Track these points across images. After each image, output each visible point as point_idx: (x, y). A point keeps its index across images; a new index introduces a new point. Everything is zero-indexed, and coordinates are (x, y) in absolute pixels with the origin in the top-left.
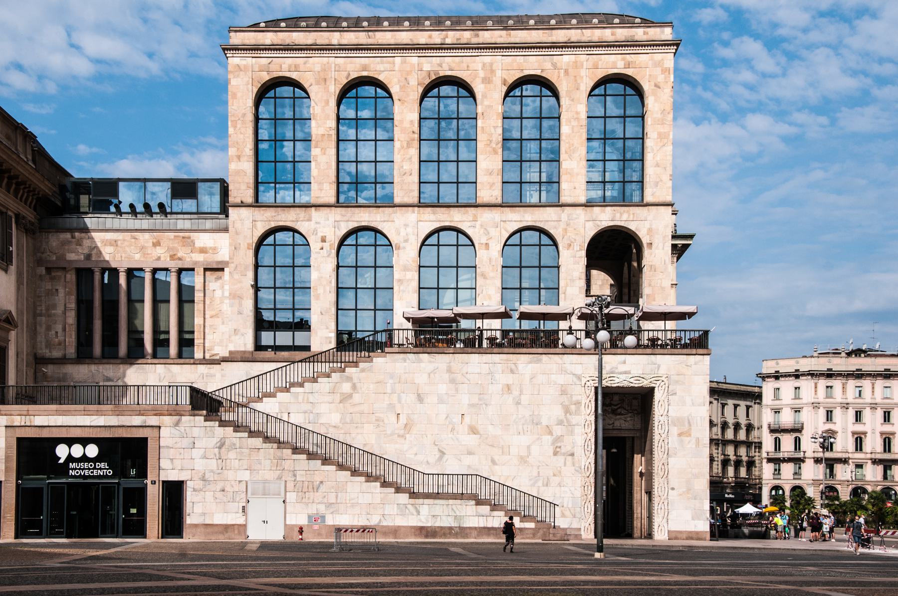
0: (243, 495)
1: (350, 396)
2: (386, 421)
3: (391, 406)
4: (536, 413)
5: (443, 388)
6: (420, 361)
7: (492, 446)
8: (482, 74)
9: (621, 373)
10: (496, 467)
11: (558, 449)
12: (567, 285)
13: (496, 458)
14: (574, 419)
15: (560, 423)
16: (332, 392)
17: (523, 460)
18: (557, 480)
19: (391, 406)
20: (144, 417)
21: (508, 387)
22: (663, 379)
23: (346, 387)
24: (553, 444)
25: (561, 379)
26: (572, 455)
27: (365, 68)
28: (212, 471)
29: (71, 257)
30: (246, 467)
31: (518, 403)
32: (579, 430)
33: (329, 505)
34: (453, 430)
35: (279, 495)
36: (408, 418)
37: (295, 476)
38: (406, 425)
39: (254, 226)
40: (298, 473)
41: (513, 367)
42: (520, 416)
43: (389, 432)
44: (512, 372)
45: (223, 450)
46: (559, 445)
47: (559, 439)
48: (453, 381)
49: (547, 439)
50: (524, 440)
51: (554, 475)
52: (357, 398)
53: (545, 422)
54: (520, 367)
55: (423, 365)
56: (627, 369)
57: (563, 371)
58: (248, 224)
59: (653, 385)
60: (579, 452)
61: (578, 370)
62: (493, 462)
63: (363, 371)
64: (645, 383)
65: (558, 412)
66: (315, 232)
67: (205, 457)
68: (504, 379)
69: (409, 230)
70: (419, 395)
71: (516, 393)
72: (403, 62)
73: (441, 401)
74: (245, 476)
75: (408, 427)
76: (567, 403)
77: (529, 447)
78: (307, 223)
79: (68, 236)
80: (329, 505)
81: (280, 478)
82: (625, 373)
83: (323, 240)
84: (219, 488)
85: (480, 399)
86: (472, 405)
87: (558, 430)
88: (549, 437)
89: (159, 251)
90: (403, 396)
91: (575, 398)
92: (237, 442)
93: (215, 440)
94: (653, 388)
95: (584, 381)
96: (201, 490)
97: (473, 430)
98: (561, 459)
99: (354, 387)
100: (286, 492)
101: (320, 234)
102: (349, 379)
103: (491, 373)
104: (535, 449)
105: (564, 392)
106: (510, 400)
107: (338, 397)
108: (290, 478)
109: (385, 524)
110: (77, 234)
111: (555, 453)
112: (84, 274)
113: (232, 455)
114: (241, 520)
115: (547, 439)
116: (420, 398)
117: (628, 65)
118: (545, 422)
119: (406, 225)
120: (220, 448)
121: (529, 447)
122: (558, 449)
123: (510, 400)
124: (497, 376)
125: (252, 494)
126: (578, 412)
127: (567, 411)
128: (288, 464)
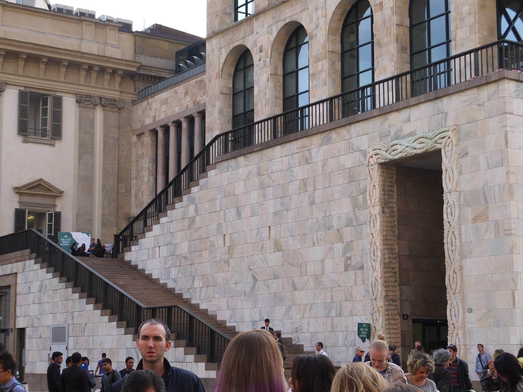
1: (193, 220)
2: (216, 246)
3: (219, 225)
4: (327, 215)
5: (254, 196)
6: (238, 167)
7: (292, 264)
9: (404, 137)
10: (296, 292)
11: (349, 262)
12: (457, 28)
13: (296, 280)
14: (363, 215)
17: (318, 278)
20: (10, 266)
21: (304, 182)
22: (450, 134)
24: (344, 253)
25: (348, 160)
26: (362, 268)
31: (312, 203)
32: (367, 230)
34: (262, 247)
35: (64, 340)
36: (232, 239)
37: (73, 318)
38: (229, 247)
39: (220, 53)
41: (308, 155)
42: (315, 220)
43: (218, 259)
44: (307, 162)
45: (42, 293)
46: (349, 255)
48: (262, 186)
49: (339, 247)
50: (316, 253)
51: (346, 300)
52: (198, 222)
53: (335, 226)
54: (314, 152)
56: (411, 129)
57: (351, 149)
58: (216, 52)
59: (438, 146)
60: (368, 264)
61: (363, 142)
64: (427, 146)
68: (300, 173)
69: (319, 13)
70: (238, 209)
71: (310, 189)
75: (230, 250)
76: (355, 194)
77: (323, 261)
78: (251, 36)
81: (66, 321)
82: (410, 134)
85: (282, 204)
86: (276, 213)
87: (348, 234)
88: (340, 244)
89: (188, 99)
91: (362, 184)
94: (439, 151)
95: (368, 156)
97: (278, 247)
98: (351, 274)
99: (196, 210)
100: (68, 337)
101: (259, 45)
103: (290, 168)
105: (351, 179)
107: (186, 222)
111: (346, 269)
116: (239, 214)
118: (335, 226)
119: (317, 9)
121: (323, 261)
122: (349, 262)
126: (365, 206)
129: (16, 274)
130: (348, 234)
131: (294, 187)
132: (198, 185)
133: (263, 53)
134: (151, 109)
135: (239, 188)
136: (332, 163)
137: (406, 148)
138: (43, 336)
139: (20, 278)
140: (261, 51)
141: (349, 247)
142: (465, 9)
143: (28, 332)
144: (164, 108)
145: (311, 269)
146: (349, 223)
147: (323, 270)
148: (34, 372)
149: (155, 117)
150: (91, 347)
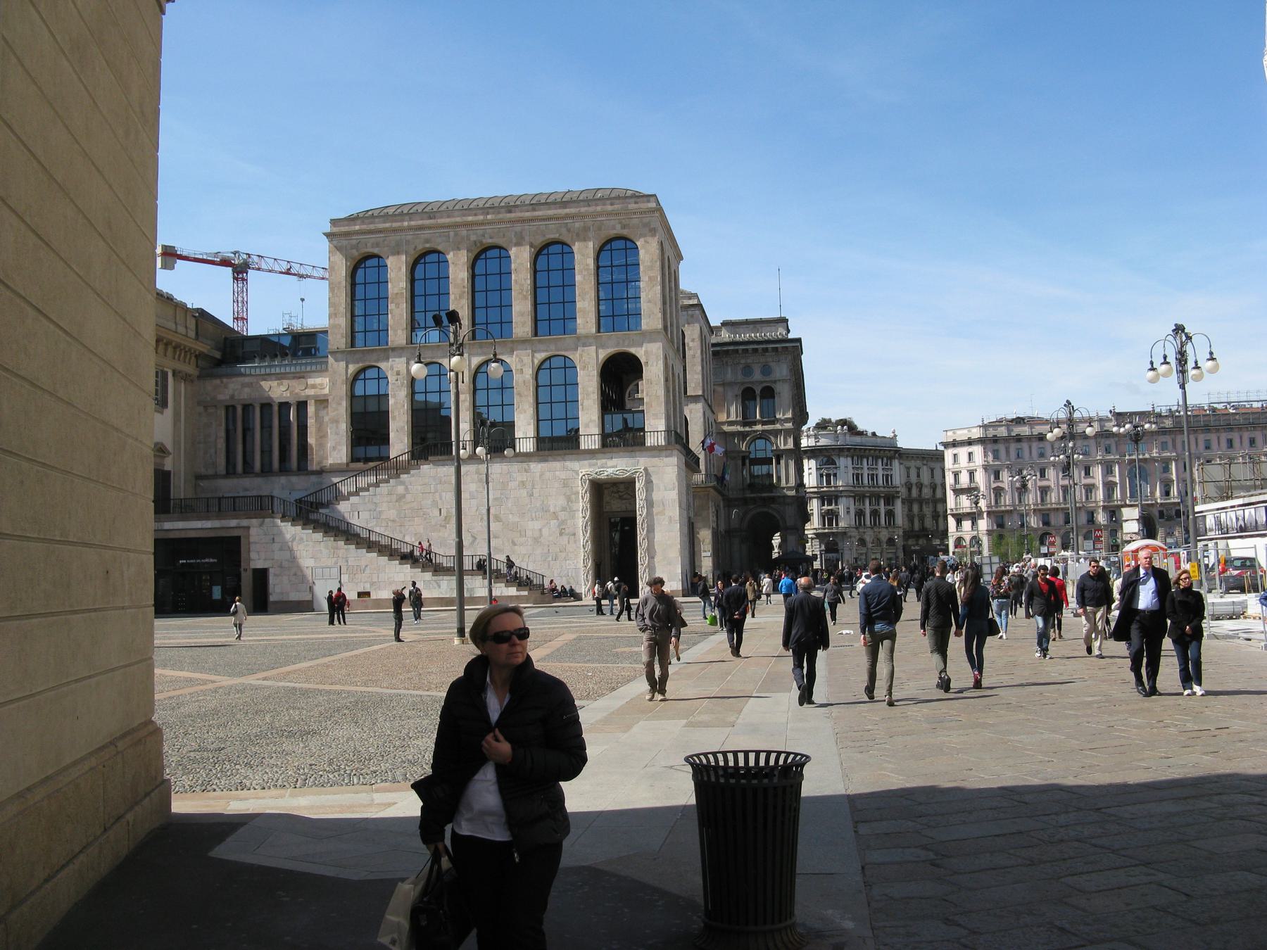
3: (435, 503)
8: (514, 240)
15: (564, 509)
16: (390, 494)
18: (563, 555)
19: (435, 503)
23: (401, 489)
25: (563, 475)
27: (427, 241)
29: (221, 397)
31: (532, 495)
44: (526, 471)
47: (563, 522)
49: (554, 523)
50: (537, 525)
52: (409, 497)
53: (552, 510)
56: (615, 466)
57: (565, 469)
62: (514, 544)
65: (562, 501)
66: (392, 368)
68: (520, 477)
72: (456, 235)
79: (218, 381)
80: (372, 584)
83: (398, 374)
87: (562, 515)
98: (565, 538)
99: (406, 489)
102: (403, 483)
104: (545, 532)
106: (524, 493)
107: (394, 498)
110: (225, 380)
111: (561, 534)
112: (230, 409)
115: (554, 523)
118: (552, 510)
123: (524, 493)
127: (569, 499)
128: (341, 553)
130: (562, 515)
134: (226, 387)
136: (548, 474)
139: (253, 531)
140: (398, 374)
141: (563, 522)
142: (591, 389)
143: (271, 571)
144: (247, 390)
145: (529, 533)
146: (564, 509)
147: (541, 535)
149: (232, 397)
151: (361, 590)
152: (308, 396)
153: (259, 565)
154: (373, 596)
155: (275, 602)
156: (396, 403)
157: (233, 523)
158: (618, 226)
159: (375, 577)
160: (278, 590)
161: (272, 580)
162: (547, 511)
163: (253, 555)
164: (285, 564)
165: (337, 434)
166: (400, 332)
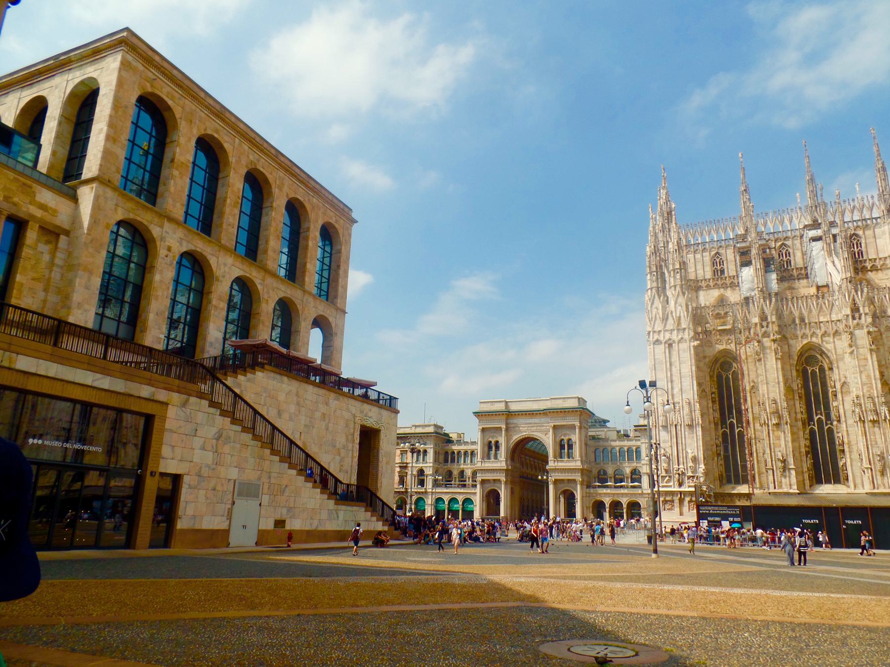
0: (230, 496)
5: (293, 408)
6: (282, 382)
20: (153, 389)
27: (217, 131)
28: (208, 466)
30: (235, 464)
31: (327, 429)
33: (290, 509)
35: (257, 496)
37: (270, 478)
40: (273, 475)
45: (220, 442)
49: (338, 458)
54: (331, 401)
55: (284, 386)
57: (348, 410)
63: (249, 380)
67: (203, 448)
68: (323, 408)
69: (227, 269)
73: (291, 419)
74: (234, 474)
80: (290, 509)
81: (259, 479)
84: (211, 485)
90: (270, 409)
92: (232, 434)
93: (214, 430)
96: (195, 488)
108: (265, 479)
109: (320, 528)
113: (227, 449)
114: (224, 526)
115: (338, 458)
117: (337, 222)
120: (217, 439)
124: (320, 406)
125: (238, 495)
129: (166, 404)
131: (318, 415)
132: (245, 376)
133: (171, 254)
135: (282, 397)
137: (371, 423)
138: (219, 488)
139: (172, 412)
143: (186, 479)
148: (197, 527)
150: (292, 505)
151: (278, 517)
152: (33, 217)
153: (170, 466)
154: (288, 527)
155: (183, 531)
156: (161, 282)
157: (145, 391)
158: (334, 219)
159: (292, 499)
160: (190, 511)
161: (185, 494)
162: (335, 446)
163: (166, 451)
164: (205, 472)
165: (87, 288)
166: (178, 205)
